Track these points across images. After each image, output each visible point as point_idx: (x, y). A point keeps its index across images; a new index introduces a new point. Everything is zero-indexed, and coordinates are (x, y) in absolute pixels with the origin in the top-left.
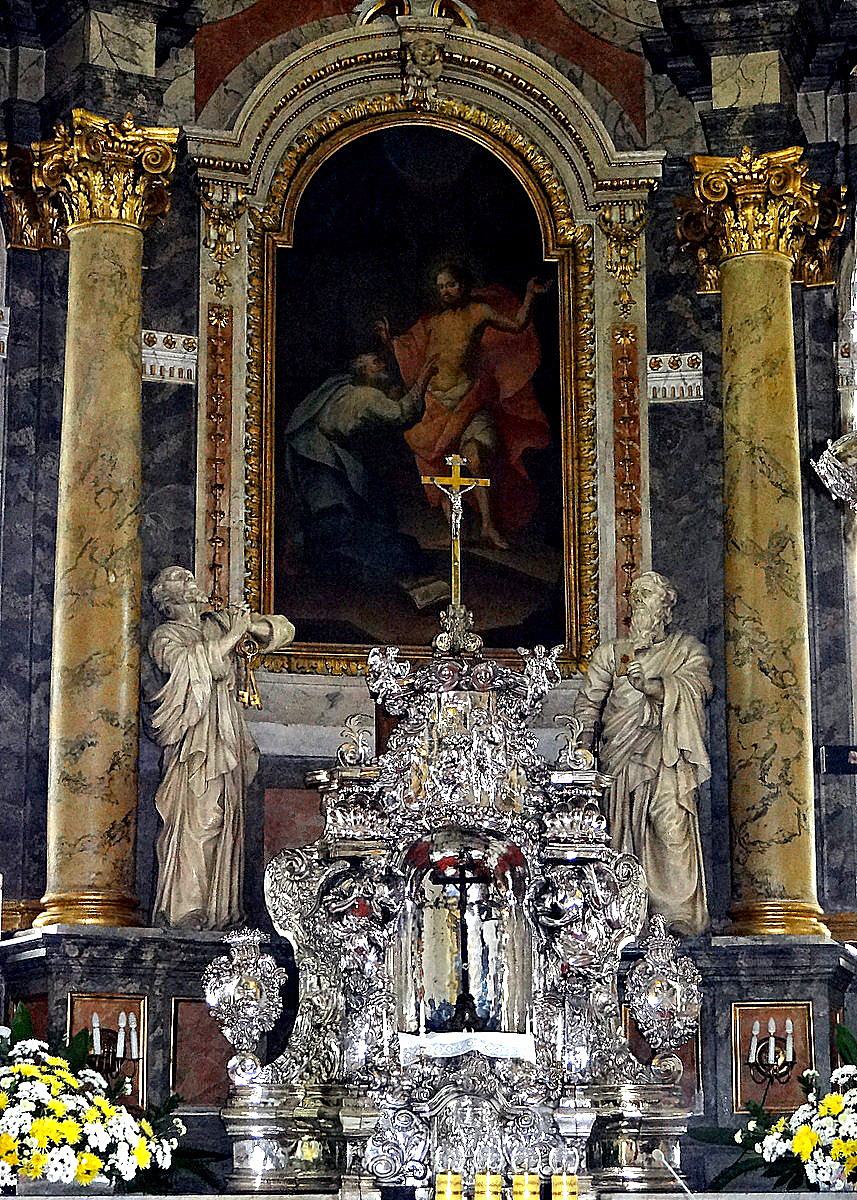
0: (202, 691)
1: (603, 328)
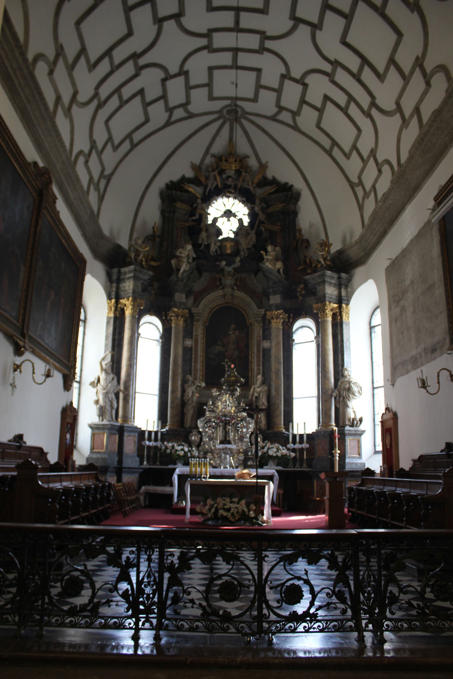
0: (190, 395)
1: (256, 336)
